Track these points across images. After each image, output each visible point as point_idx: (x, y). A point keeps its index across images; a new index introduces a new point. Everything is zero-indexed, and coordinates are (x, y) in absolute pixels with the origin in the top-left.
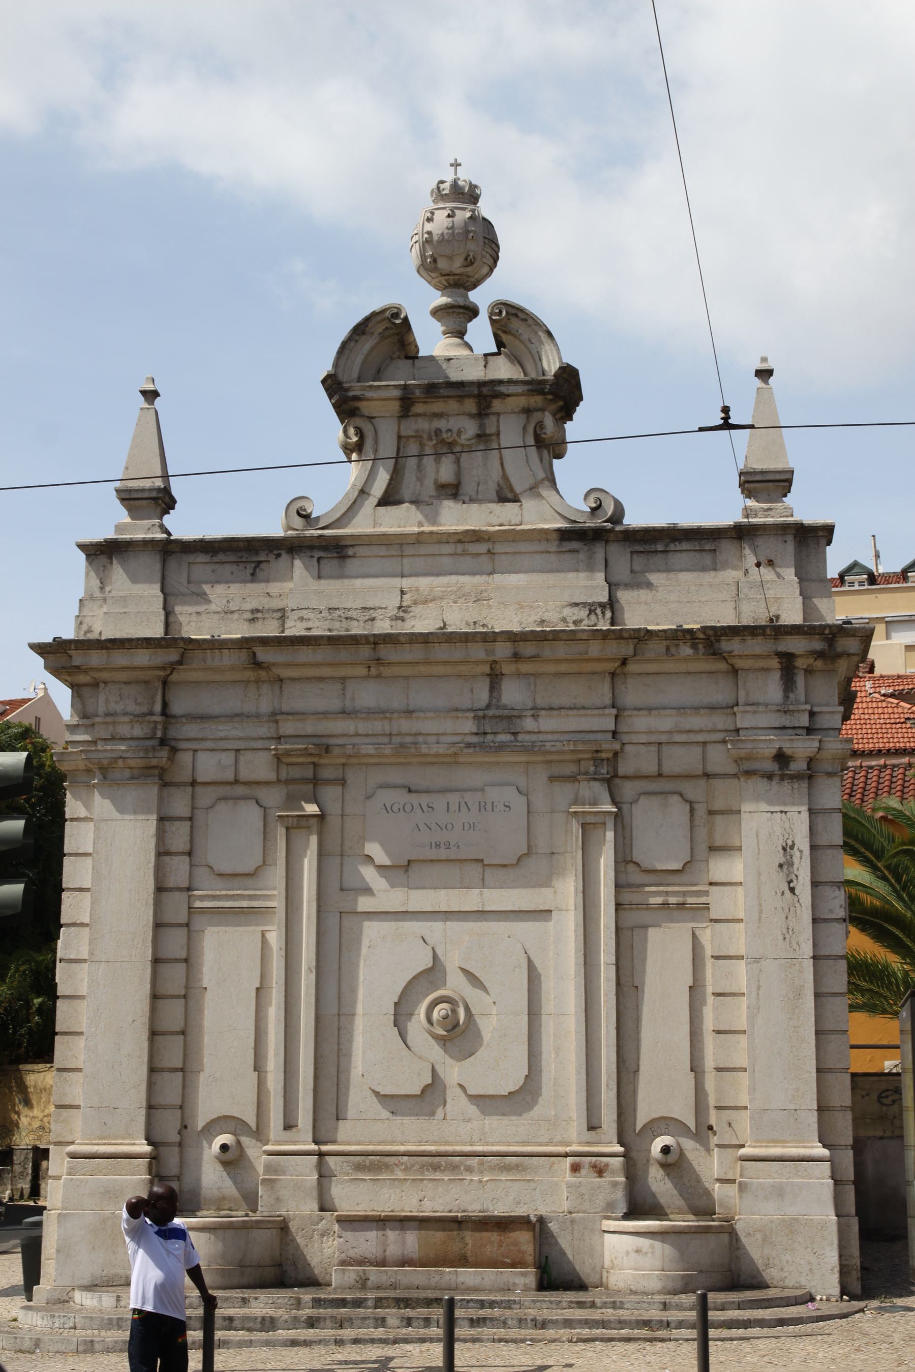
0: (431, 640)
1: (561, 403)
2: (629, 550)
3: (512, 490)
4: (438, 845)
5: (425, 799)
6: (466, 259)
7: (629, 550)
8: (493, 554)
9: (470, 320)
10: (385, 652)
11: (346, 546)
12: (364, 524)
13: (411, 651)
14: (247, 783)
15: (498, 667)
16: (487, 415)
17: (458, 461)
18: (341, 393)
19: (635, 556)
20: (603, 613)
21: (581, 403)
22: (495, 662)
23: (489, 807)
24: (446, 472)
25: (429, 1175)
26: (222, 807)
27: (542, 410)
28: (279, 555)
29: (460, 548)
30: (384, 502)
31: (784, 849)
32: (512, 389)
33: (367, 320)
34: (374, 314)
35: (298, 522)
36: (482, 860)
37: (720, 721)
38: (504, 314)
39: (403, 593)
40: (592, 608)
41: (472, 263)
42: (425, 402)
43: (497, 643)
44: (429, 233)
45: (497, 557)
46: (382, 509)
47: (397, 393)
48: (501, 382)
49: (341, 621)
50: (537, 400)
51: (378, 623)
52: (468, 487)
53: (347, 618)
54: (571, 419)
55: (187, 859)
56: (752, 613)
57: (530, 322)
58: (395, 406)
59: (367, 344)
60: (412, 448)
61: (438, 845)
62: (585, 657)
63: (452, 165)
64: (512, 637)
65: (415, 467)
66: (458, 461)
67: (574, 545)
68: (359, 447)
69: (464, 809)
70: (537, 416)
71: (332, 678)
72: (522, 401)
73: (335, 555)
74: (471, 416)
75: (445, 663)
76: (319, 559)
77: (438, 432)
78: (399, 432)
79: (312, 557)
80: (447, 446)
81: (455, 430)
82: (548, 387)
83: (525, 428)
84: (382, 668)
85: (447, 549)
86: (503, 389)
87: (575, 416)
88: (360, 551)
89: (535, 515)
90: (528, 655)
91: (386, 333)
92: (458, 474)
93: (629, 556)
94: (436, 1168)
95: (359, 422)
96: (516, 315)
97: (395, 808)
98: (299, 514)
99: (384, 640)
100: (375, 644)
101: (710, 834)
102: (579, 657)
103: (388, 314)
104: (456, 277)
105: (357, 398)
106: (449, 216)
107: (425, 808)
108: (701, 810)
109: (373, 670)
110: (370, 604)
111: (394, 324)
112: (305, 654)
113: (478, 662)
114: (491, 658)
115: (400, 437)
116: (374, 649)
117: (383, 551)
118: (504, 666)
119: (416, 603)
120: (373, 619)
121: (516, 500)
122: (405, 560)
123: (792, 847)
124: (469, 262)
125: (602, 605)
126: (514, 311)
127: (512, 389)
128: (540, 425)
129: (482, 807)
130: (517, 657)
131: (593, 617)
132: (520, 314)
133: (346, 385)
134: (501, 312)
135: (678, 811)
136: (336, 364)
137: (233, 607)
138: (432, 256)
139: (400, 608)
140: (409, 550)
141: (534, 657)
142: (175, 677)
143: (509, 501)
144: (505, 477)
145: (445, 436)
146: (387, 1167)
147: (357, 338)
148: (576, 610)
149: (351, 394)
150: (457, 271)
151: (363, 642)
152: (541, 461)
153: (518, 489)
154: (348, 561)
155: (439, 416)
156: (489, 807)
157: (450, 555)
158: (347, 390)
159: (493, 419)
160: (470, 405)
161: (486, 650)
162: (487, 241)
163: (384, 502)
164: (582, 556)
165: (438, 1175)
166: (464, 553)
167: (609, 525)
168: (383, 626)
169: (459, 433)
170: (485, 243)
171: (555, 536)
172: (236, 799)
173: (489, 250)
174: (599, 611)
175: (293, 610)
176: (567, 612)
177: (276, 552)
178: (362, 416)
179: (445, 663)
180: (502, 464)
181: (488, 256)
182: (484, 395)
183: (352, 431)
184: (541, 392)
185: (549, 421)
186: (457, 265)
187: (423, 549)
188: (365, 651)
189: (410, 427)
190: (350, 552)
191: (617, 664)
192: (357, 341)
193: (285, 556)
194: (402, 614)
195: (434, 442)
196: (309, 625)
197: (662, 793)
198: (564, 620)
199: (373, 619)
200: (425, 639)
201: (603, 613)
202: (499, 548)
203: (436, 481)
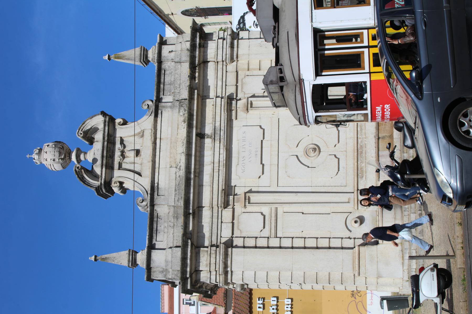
4: (256, 155)
5: (241, 159)
14: (233, 219)
23: (244, 138)
25: (364, 155)
26: (240, 227)
31: (261, 46)
36: (262, 141)
37: (220, 66)
38: (81, 132)
40: (181, 106)
41: (63, 147)
51: (181, 174)
55: (258, 239)
56: (186, 57)
61: (256, 155)
69: (244, 147)
71: (199, 189)
94: (362, 153)
97: (243, 169)
98: (142, 202)
101: (255, 69)
107: (244, 159)
108: (248, 73)
123: (260, 44)
129: (244, 141)
131: (184, 105)
135: (248, 79)
137: (172, 225)
139: (176, 167)
142: (195, 243)
143: (143, 134)
146: (361, 168)
148: (181, 111)
156: (244, 138)
165: (364, 152)
172: (238, 222)
194: (178, 167)
196: (180, 198)
197: (242, 85)
198: (184, 114)
199: (180, 176)
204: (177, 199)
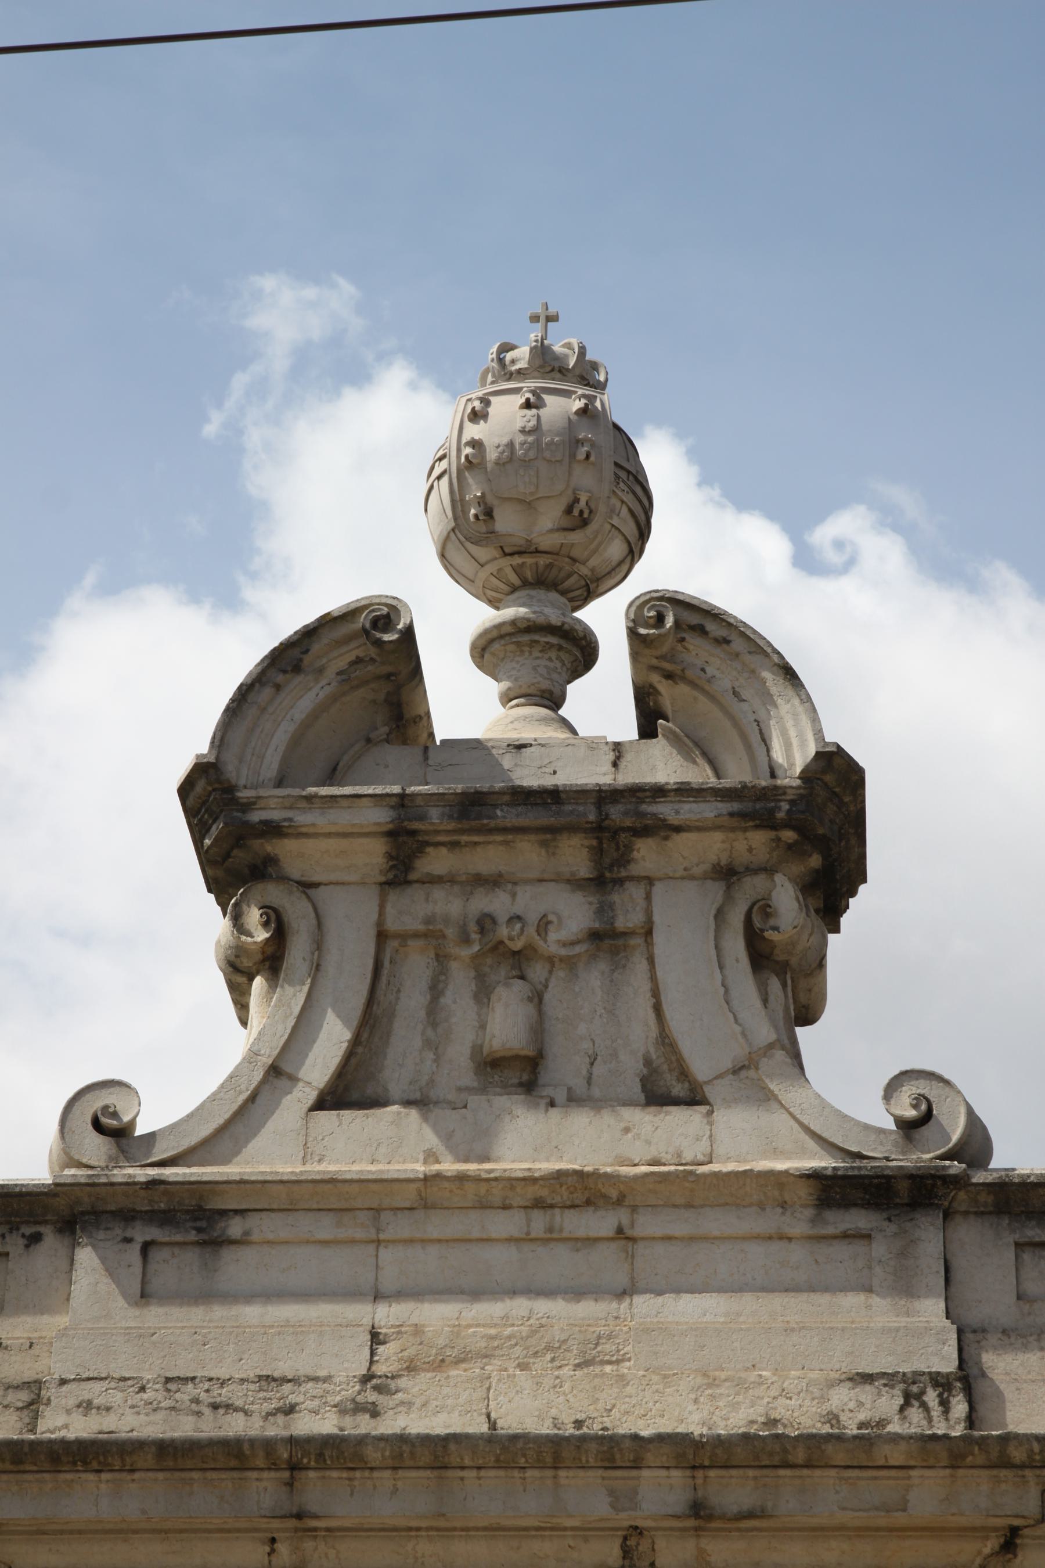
0: (455, 1460)
1: (815, 861)
2: (1010, 1239)
3: (684, 1074)
6: (569, 510)
7: (1010, 1239)
8: (633, 1240)
9: (569, 682)
10: (318, 1490)
11: (224, 1213)
12: (273, 1154)
13: (395, 1490)
15: (644, 1546)
16: (620, 882)
17: (537, 998)
18: (229, 821)
19: (1026, 1256)
20: (945, 1404)
21: (862, 888)
22: (637, 1531)
24: (506, 1025)
27: (768, 870)
28: (35, 1239)
29: (539, 1221)
30: (336, 1097)
32: (689, 811)
33: (309, 634)
34: (327, 622)
35: (95, 1149)
39: (376, 1338)
40: (911, 1389)
41: (584, 522)
42: (454, 845)
43: (645, 1473)
44: (475, 444)
45: (640, 1248)
46: (327, 1118)
47: (380, 817)
48: (659, 792)
49: (199, 1414)
50: (756, 843)
52: (564, 1067)
53: (215, 1407)
54: (836, 930)
57: (738, 645)
58: (372, 855)
59: (304, 699)
60: (415, 969)
62: (900, 1519)
63: (535, 319)
64: (691, 1453)
65: (422, 1014)
66: (537, 998)
67: (859, 1219)
68: (272, 961)
70: (751, 887)
72: (714, 847)
73: (193, 1236)
74: (576, 884)
75: (494, 1530)
76: (146, 1248)
77: (486, 922)
78: (380, 923)
79: (128, 1240)
80: (508, 958)
81: (533, 918)
82: (785, 806)
83: (720, 916)
84: (309, 1545)
85: (504, 1224)
86: (664, 810)
87: (845, 920)
88: (263, 1227)
89: (744, 1141)
90: (735, 1509)
91: (352, 669)
92: (538, 1029)
93: (1010, 1254)
95: (274, 893)
96: (700, 630)
98: (97, 1126)
99: (320, 1456)
100: (294, 1467)
102: (882, 1521)
103: (363, 620)
104: (543, 561)
105: (273, 830)
106: (528, 405)
109: (282, 1548)
110: (283, 1368)
111: (379, 643)
112: (89, 1498)
113: (586, 1531)
114: (625, 1519)
115: (382, 936)
116: (290, 1484)
117: (325, 1228)
118: (661, 1544)
119: (411, 1368)
120: (290, 1410)
121: (695, 1098)
122: (386, 1255)
124: (578, 518)
125: (941, 1382)
126: (694, 619)
127: (689, 811)
128: (763, 908)
130: (700, 1513)
132: (711, 627)
133: (243, 794)
134: (660, 619)
136: (221, 737)
138: (481, 501)
139: (367, 1378)
140: (398, 1227)
141: (750, 1515)
144: (665, 1040)
145: (503, 932)
147: (280, 678)
148: (865, 1393)
149: (255, 817)
150: (547, 542)
151: (260, 1462)
152: (765, 1001)
153: (701, 1068)
154: (228, 1254)
155: (493, 882)
157: (510, 1240)
158: (248, 806)
159: (636, 891)
160: (575, 855)
161: (611, 1492)
162: (623, 475)
163: (336, 1097)
164: (879, 1249)
166: (551, 1238)
167: (956, 1167)
168: (318, 1422)
169: (544, 925)
170: (617, 477)
171: (804, 1192)
173: (629, 498)
174: (931, 1397)
175: (63, 1382)
176: (841, 1398)
177: (28, 1230)
178: (283, 879)
179: (494, 1530)
180: (658, 1009)
181: (624, 510)
182: (610, 825)
183: (254, 916)
184: (766, 821)
185: (786, 899)
186: (544, 525)
187: (436, 1226)
188: (264, 1489)
189: (409, 910)
190: (235, 1228)
191: (991, 1545)
192: (278, 687)
193: (51, 1240)
194: (372, 1396)
195: (476, 948)
199: (290, 1410)
200: (438, 1454)
201: (945, 1404)
202: (647, 1225)
203: (476, 1050)
204: (93, 1391)
